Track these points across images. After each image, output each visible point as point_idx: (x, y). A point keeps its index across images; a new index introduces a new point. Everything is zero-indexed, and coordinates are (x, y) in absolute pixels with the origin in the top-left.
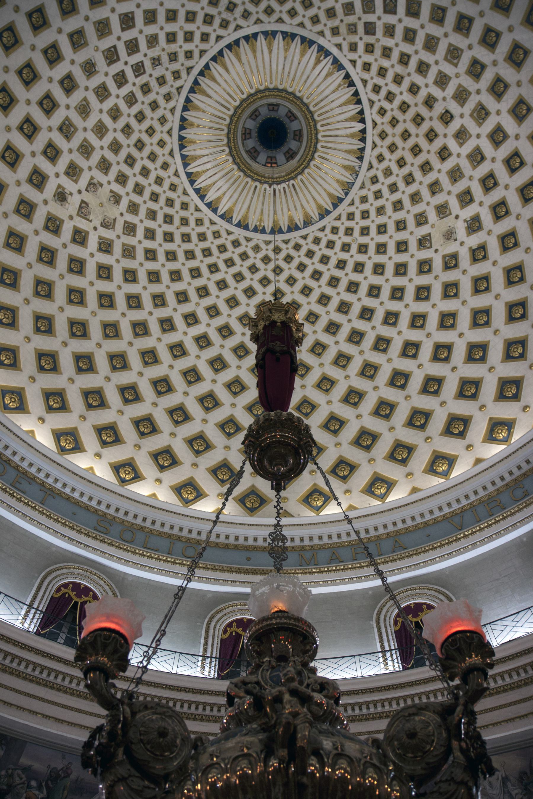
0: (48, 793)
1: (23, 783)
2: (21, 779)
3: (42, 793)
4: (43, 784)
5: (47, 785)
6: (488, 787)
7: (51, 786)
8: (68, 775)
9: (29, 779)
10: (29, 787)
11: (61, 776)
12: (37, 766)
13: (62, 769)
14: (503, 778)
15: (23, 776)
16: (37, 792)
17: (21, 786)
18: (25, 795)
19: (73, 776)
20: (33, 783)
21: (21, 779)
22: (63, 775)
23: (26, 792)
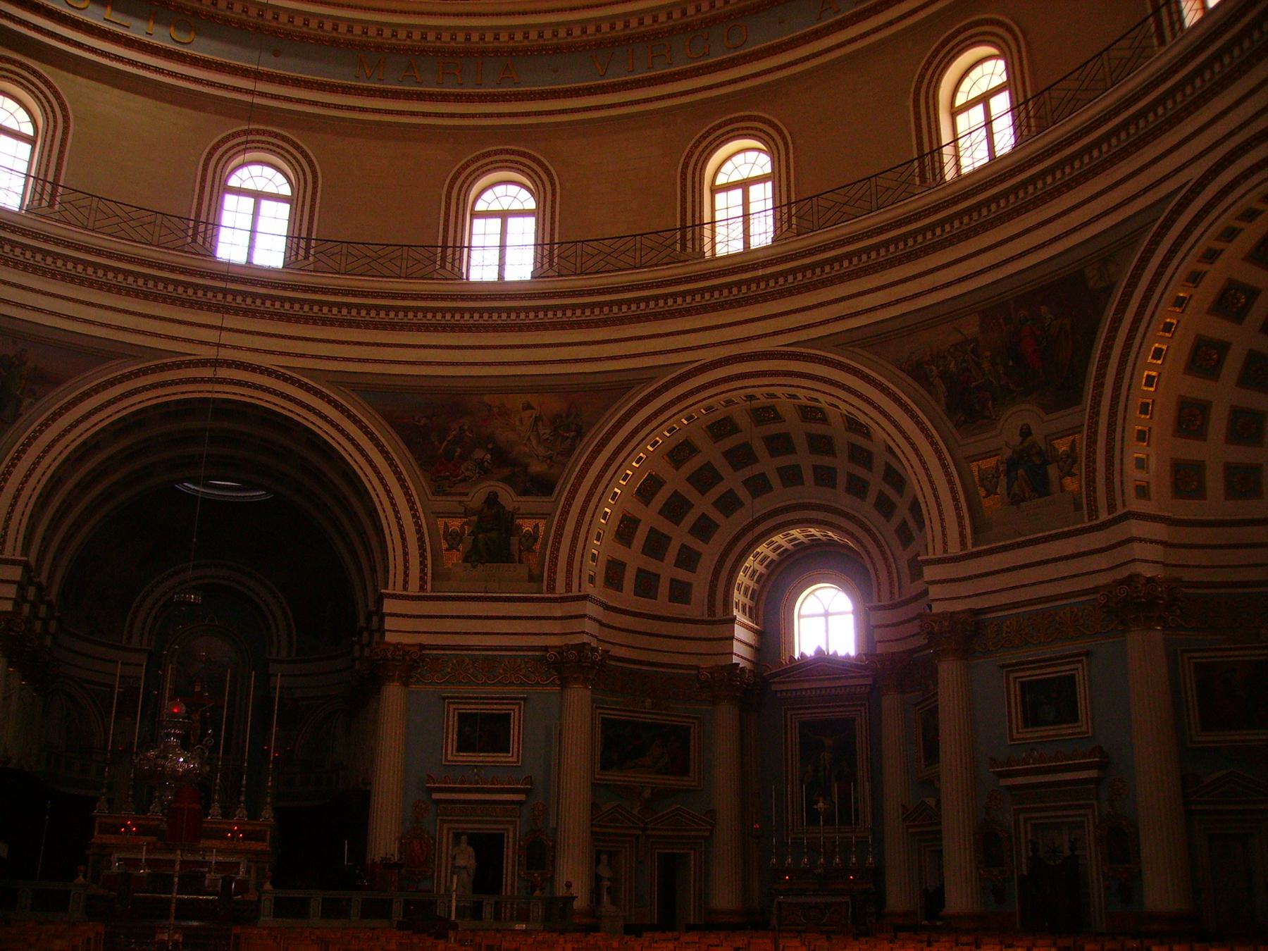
6: (517, 424)
13: (15, 356)
14: (536, 417)
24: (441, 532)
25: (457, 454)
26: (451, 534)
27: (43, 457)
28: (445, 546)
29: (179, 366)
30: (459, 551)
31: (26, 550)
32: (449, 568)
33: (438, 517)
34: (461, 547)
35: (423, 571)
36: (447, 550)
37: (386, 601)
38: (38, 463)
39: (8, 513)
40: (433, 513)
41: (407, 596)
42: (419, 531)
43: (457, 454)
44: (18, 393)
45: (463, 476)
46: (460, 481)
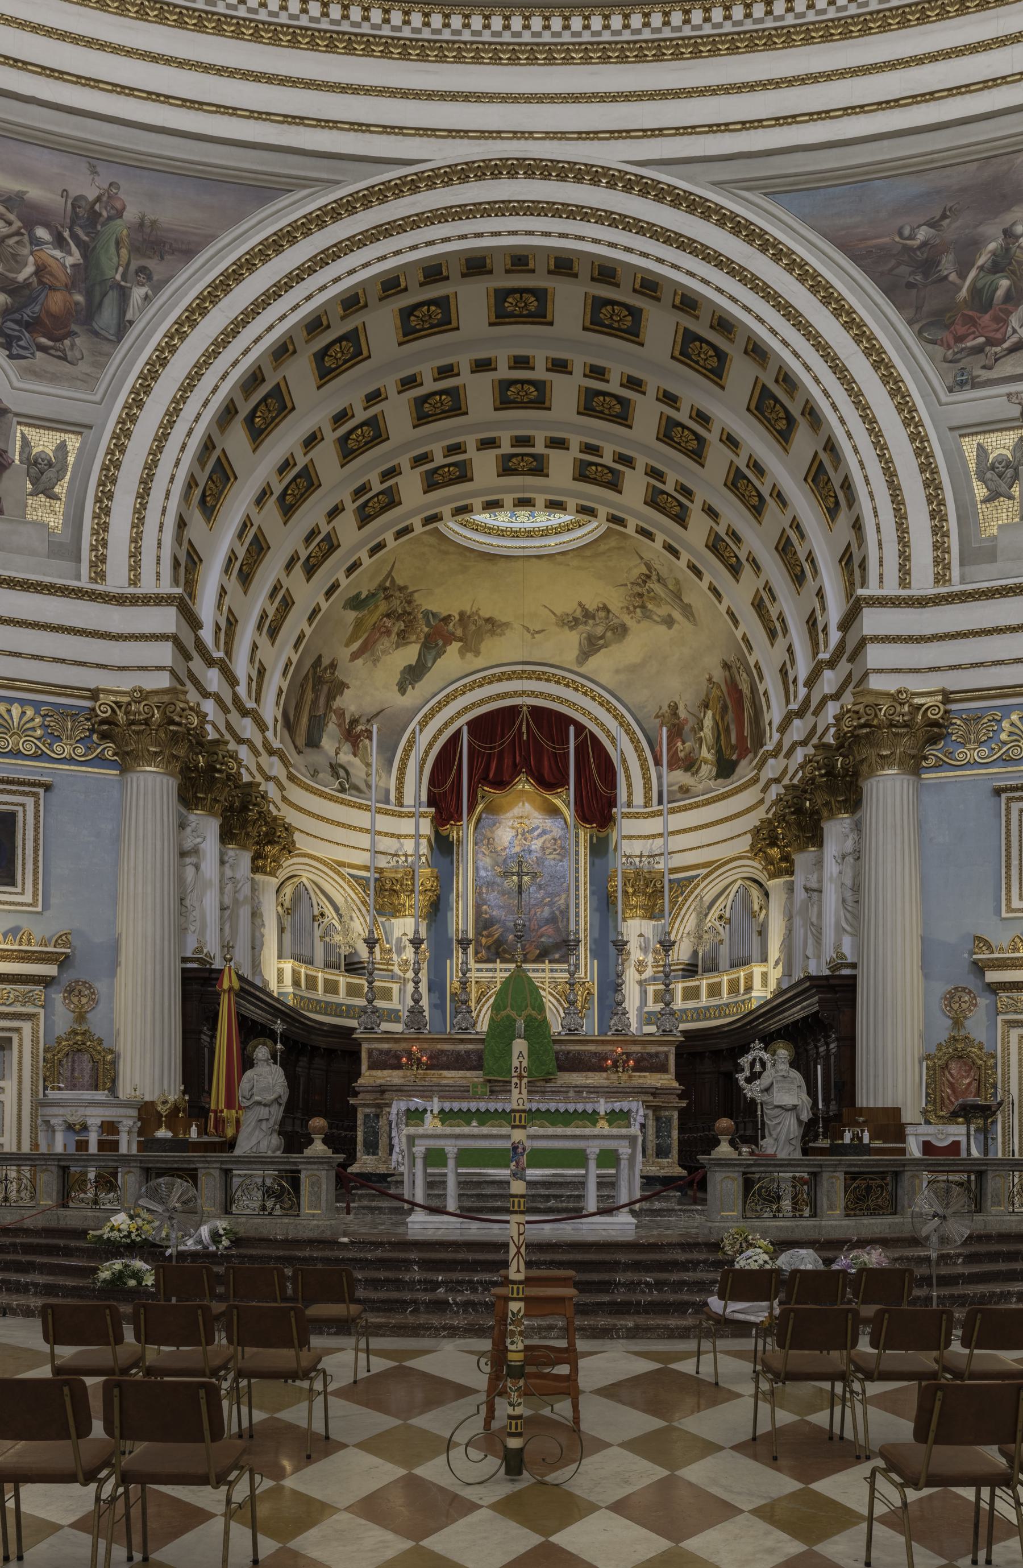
0: (84, 256)
1: (18, 233)
2: (9, 223)
3: (70, 253)
4: (66, 234)
5: (74, 236)
7: (86, 238)
8: (120, 214)
9: (29, 225)
10: (35, 241)
11: (100, 215)
12: (35, 193)
13: (98, 199)
15: (12, 217)
16: (57, 253)
17: (16, 239)
18: (31, 259)
19: (131, 214)
20: (41, 233)
21: (9, 223)
22: (105, 214)
23: (32, 253)
24: (972, 466)
25: (1000, 293)
26: (993, 468)
27: (184, 399)
28: (980, 491)
29: (412, 185)
30: (1011, 497)
31: (176, 582)
32: (993, 538)
33: (962, 436)
34: (1016, 490)
35: (940, 547)
36: (985, 501)
37: (866, 612)
38: (177, 411)
39: (136, 511)
40: (952, 429)
41: (911, 598)
42: (927, 466)
43: (1000, 293)
44: (118, 277)
45: (1014, 339)
46: (1012, 350)
